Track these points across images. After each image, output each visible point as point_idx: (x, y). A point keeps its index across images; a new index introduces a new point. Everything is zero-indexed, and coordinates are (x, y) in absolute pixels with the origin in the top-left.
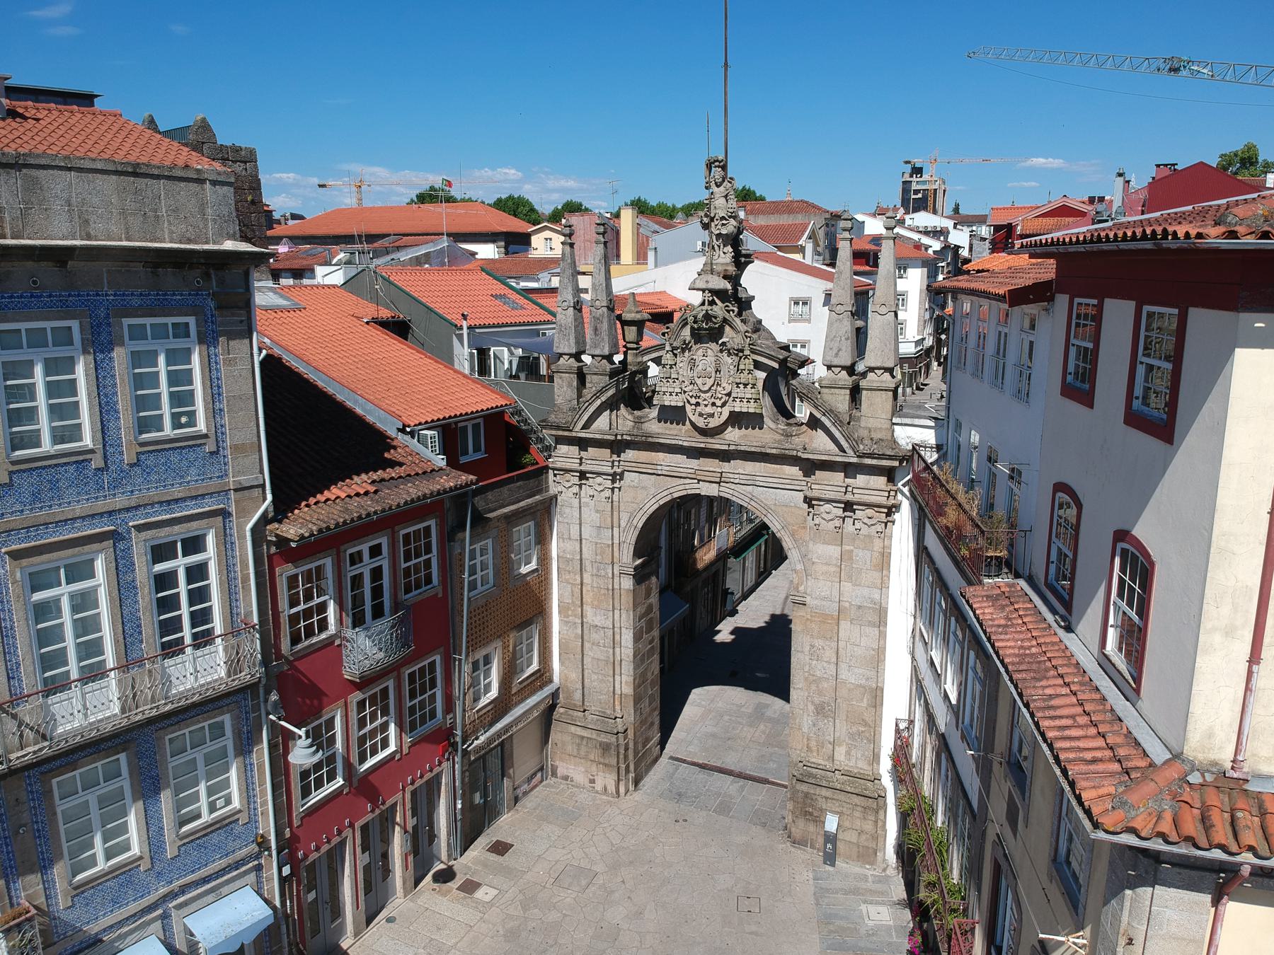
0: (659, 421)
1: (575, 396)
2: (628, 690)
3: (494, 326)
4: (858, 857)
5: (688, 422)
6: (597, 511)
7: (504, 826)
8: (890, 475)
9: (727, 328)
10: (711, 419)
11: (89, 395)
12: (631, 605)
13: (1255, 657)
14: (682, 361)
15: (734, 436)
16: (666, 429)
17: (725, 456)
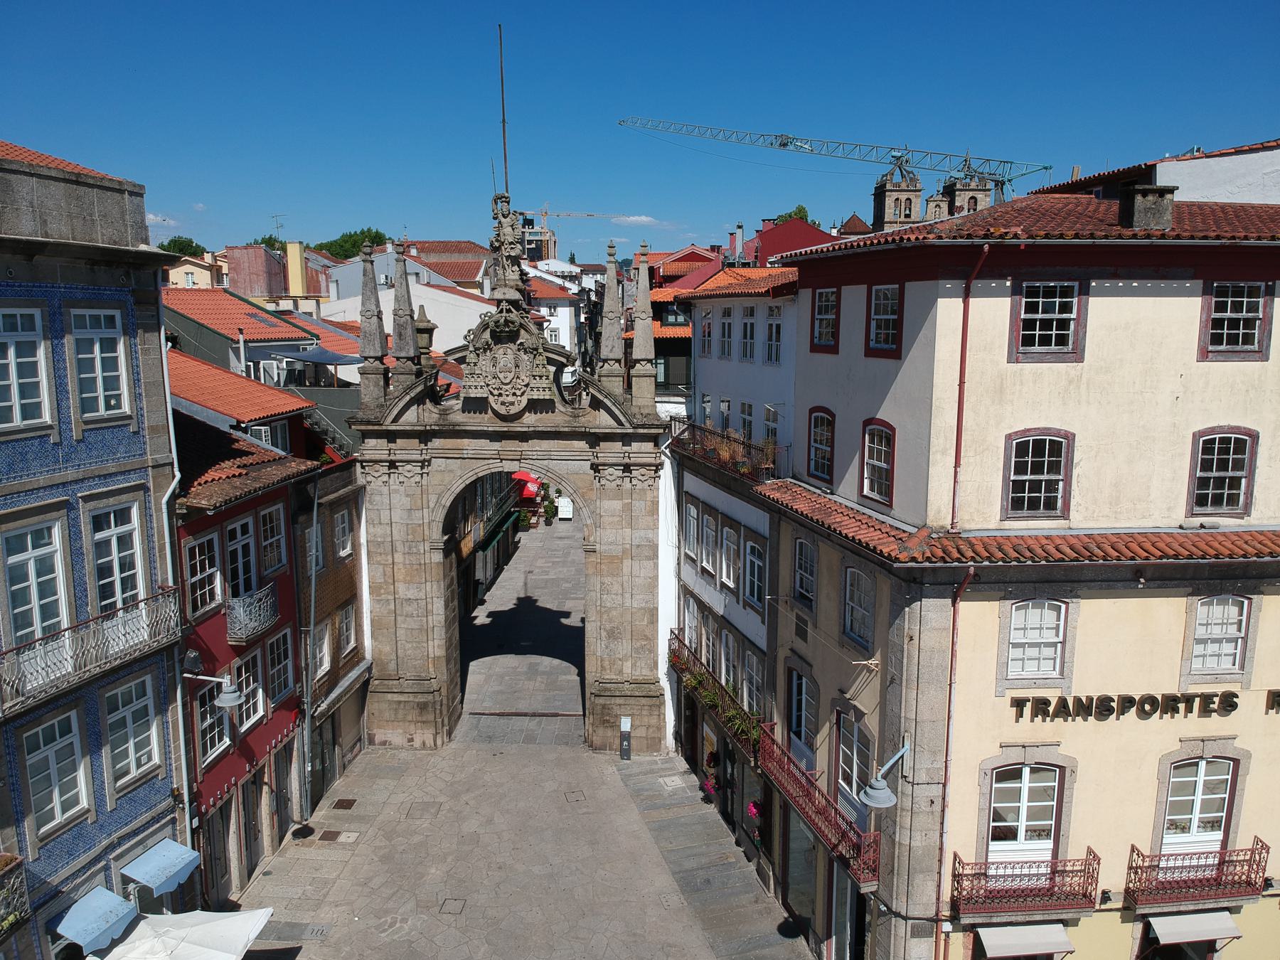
0: (463, 412)
1: (382, 394)
2: (441, 652)
3: (261, 341)
4: (648, 748)
5: (490, 411)
6: (407, 496)
7: (339, 787)
8: (655, 440)
9: (522, 332)
10: (511, 407)
11: (48, 376)
12: (442, 576)
13: (957, 463)
15: (530, 420)
16: (470, 418)
17: (524, 437)
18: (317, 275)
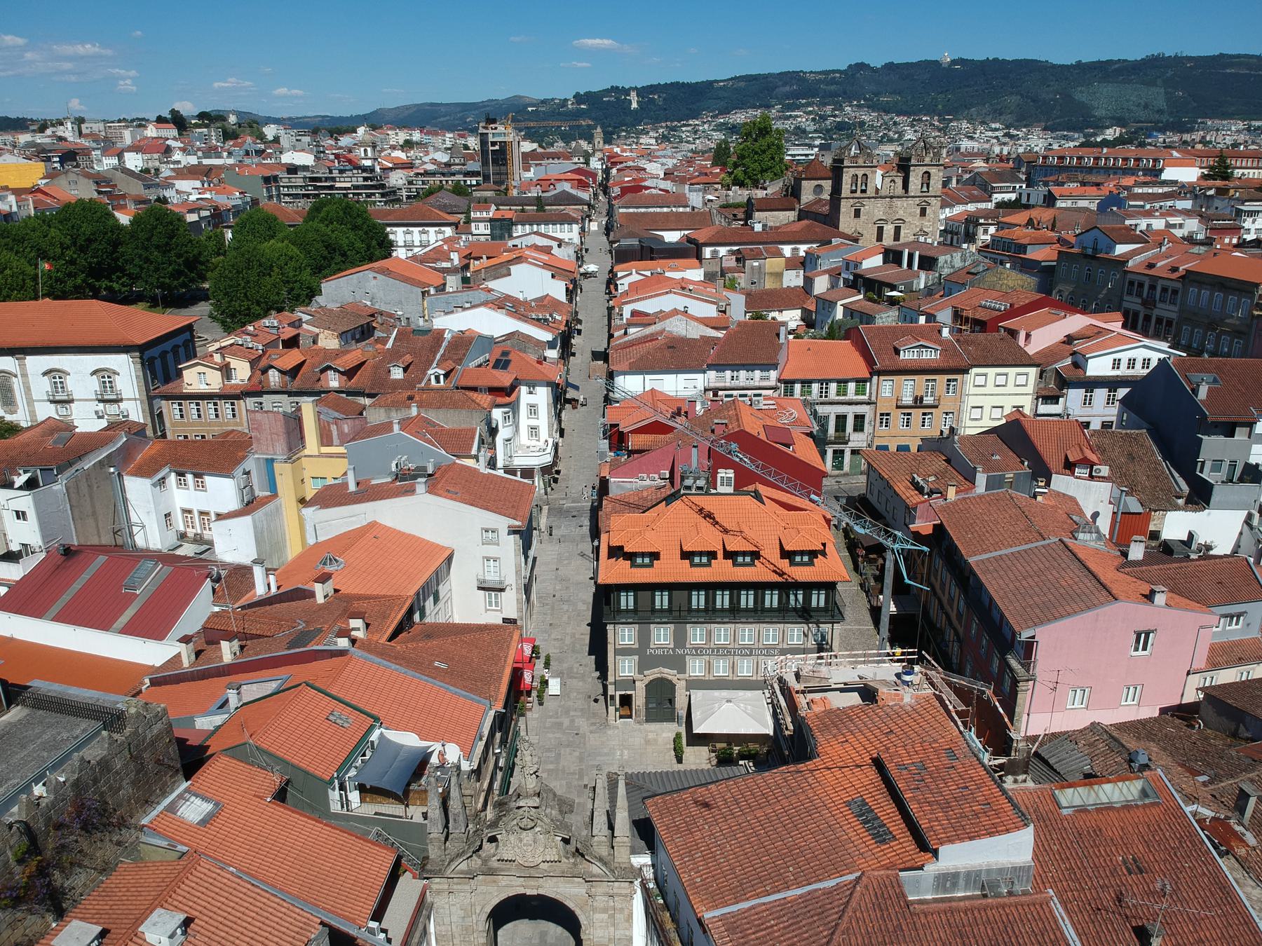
14: (512, 838)
18: (329, 425)
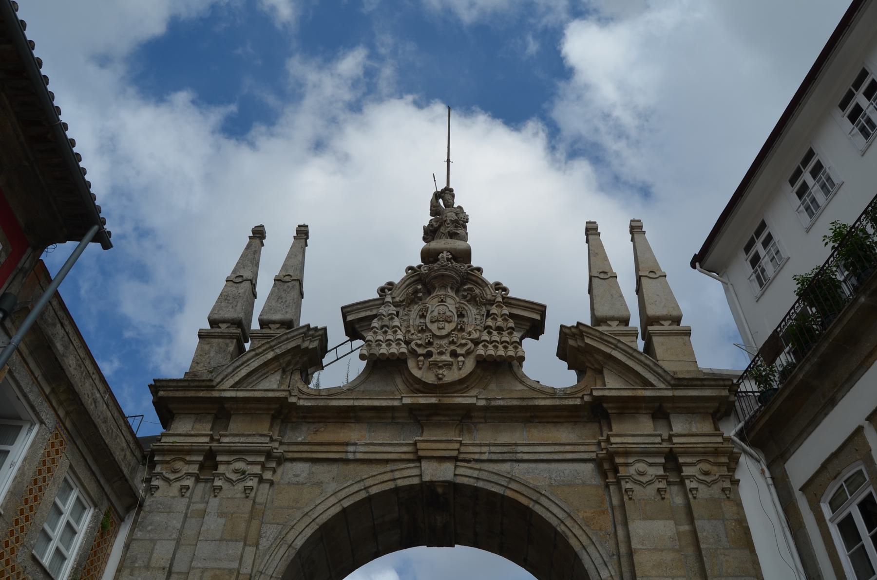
10: (445, 371)
